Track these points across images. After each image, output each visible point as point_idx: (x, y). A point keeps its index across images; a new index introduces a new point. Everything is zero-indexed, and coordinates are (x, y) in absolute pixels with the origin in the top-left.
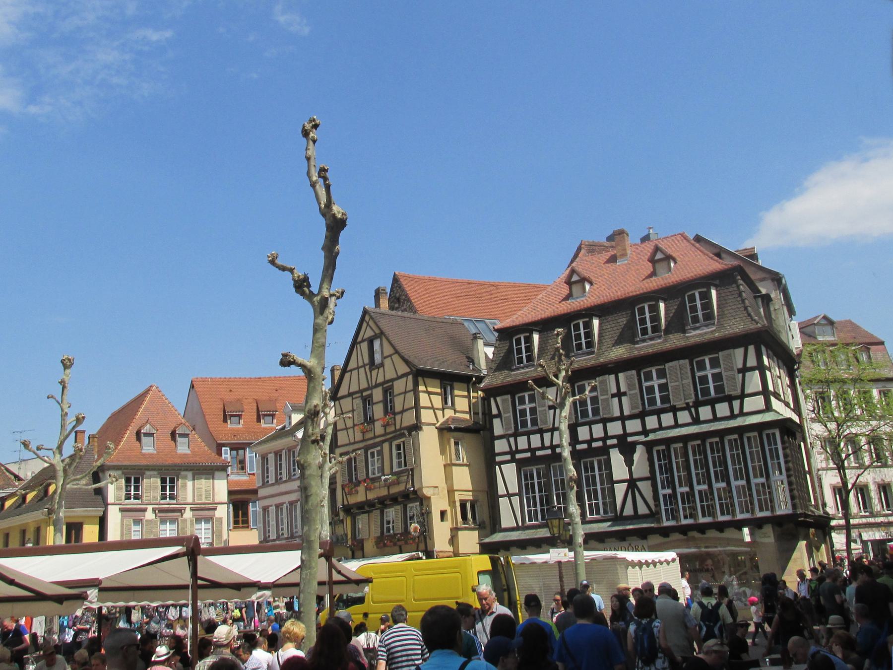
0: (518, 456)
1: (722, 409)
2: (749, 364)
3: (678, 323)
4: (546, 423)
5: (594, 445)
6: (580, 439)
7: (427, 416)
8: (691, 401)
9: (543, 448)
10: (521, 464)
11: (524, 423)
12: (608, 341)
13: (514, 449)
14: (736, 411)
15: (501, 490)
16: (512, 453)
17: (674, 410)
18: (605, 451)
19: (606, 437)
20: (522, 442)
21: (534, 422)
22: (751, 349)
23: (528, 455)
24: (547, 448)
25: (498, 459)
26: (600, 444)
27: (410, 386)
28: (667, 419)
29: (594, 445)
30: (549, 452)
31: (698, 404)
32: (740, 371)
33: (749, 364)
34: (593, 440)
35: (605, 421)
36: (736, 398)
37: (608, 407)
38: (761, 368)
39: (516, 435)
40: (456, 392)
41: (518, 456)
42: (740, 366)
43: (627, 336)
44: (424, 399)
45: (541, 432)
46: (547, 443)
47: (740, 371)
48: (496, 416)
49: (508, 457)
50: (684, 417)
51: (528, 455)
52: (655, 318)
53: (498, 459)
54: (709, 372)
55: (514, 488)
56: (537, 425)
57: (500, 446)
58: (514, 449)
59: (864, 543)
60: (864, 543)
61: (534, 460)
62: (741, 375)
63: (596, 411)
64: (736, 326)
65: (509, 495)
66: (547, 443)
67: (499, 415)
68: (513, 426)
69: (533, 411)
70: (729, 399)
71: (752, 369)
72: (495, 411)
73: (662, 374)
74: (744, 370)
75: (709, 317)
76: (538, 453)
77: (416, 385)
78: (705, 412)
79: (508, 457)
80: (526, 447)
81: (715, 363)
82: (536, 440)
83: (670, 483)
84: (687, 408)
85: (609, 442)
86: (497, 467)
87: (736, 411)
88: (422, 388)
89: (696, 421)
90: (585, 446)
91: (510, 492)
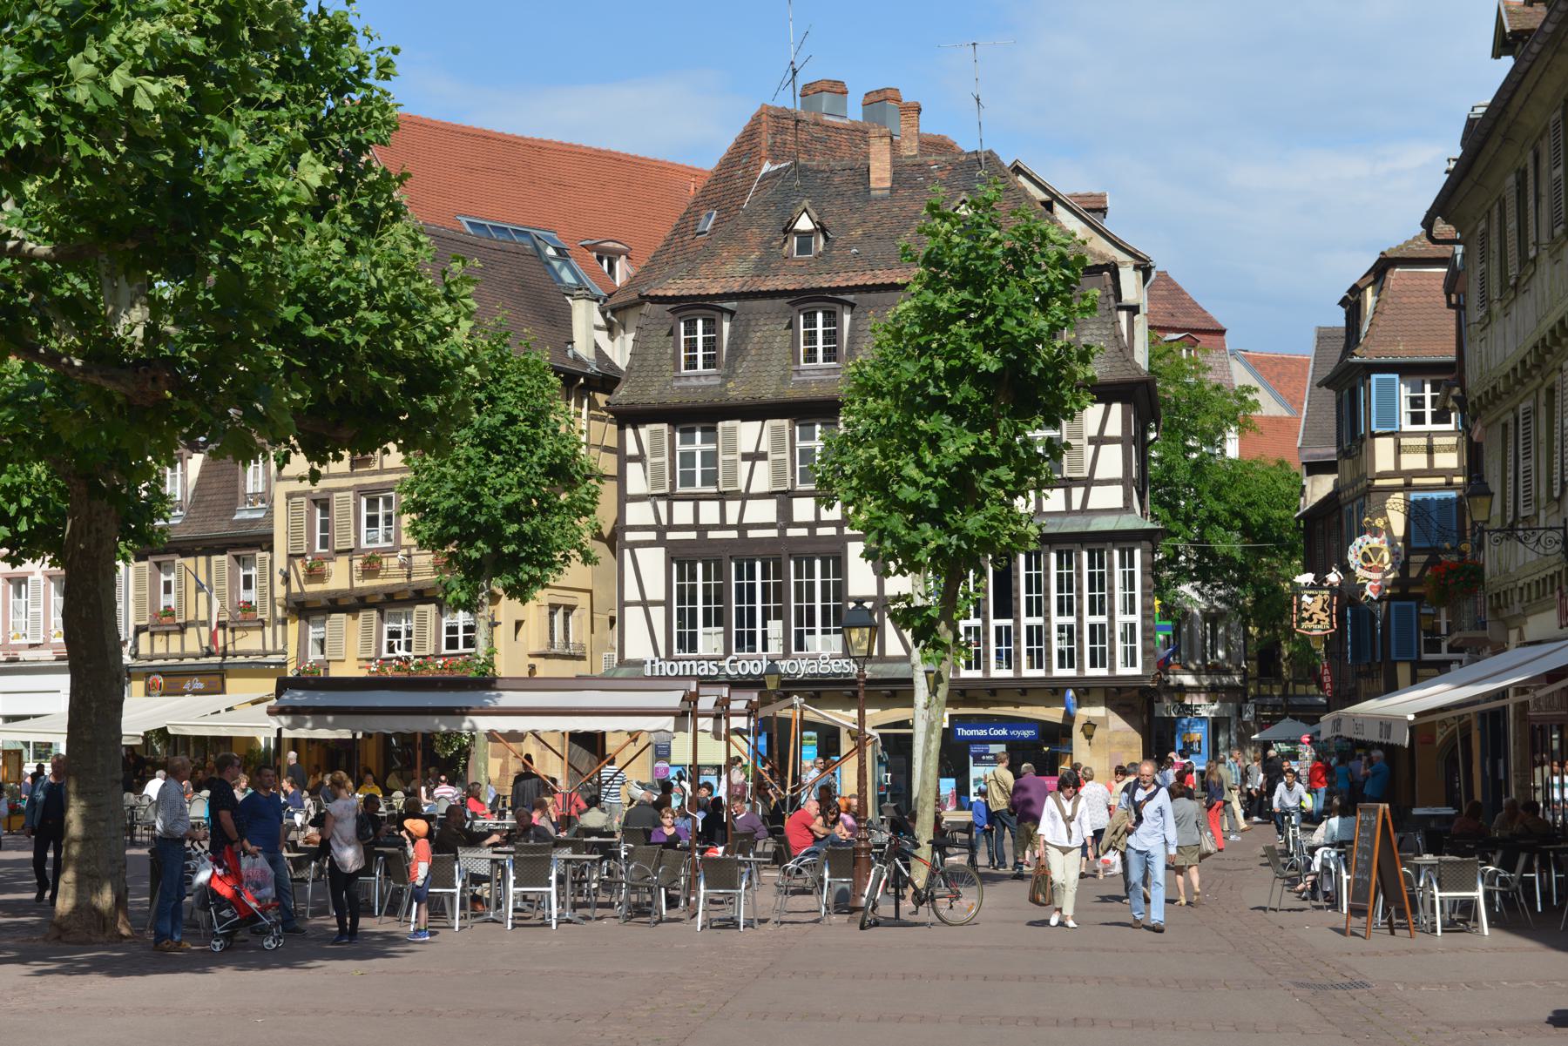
0: (671, 536)
2: (1108, 432)
4: (734, 482)
5: (821, 531)
6: (797, 518)
9: (723, 526)
11: (688, 479)
13: (664, 521)
14: (1076, 505)
16: (660, 529)
20: (683, 513)
21: (710, 479)
23: (693, 535)
24: (731, 527)
26: (832, 531)
29: (821, 531)
30: (734, 534)
32: (1091, 441)
33: (1108, 432)
34: (819, 523)
39: (671, 498)
41: (671, 536)
42: (1093, 431)
45: (722, 497)
46: (732, 519)
47: (1091, 441)
49: (652, 536)
51: (693, 535)
53: (630, 536)
55: (656, 591)
56: (716, 483)
58: (664, 521)
62: (1092, 448)
65: (645, 604)
66: (732, 519)
67: (640, 458)
68: (667, 480)
69: (710, 458)
76: (712, 535)
79: (652, 536)
80: (690, 521)
82: (710, 512)
86: (627, 552)
87: (1076, 505)
90: (804, 532)
91: (649, 597)
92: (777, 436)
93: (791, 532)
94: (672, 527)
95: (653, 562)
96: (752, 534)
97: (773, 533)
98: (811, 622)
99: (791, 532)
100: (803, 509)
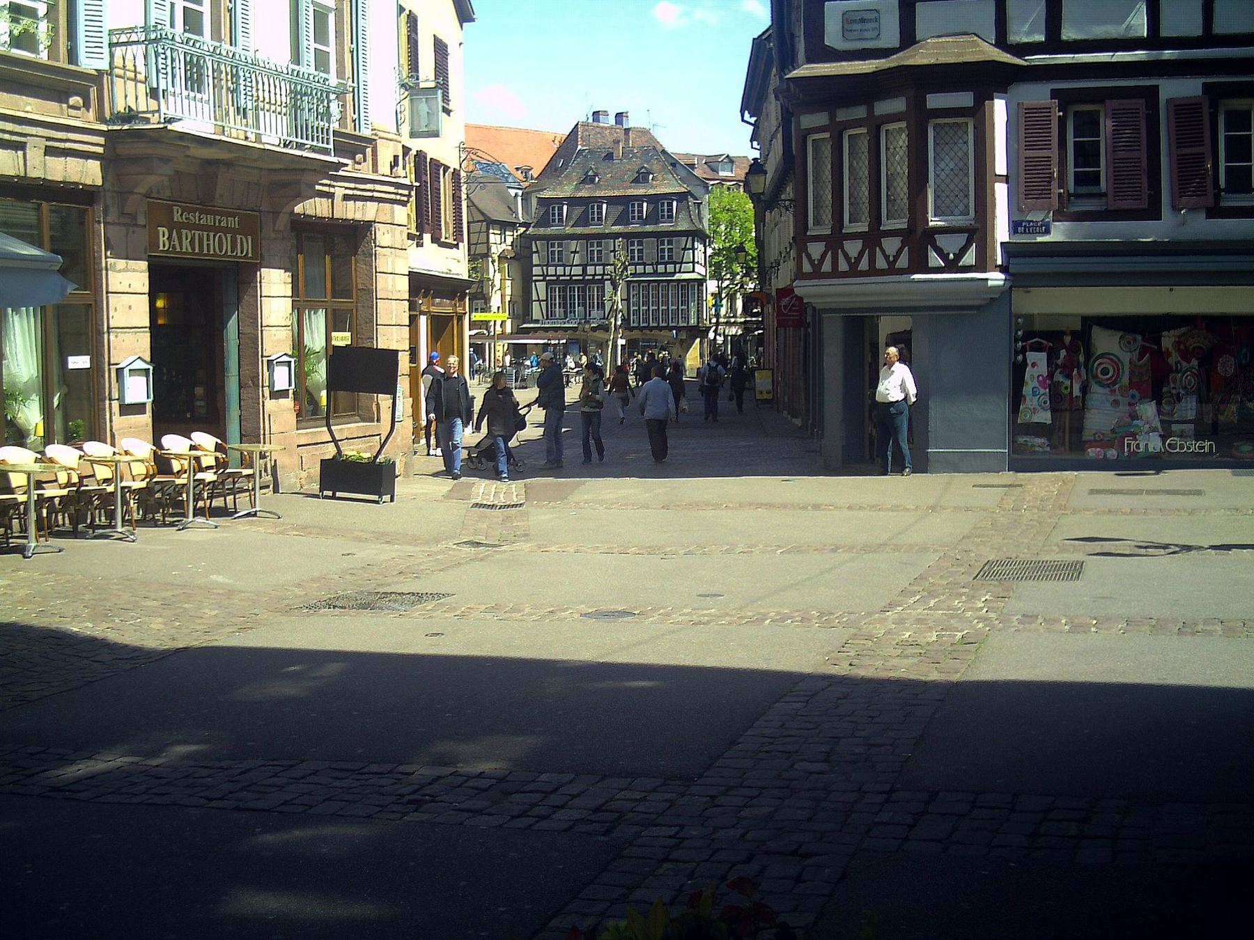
0: (548, 278)
1: (670, 268)
3: (654, 218)
5: (596, 277)
7: (494, 249)
8: (654, 262)
9: (564, 275)
10: (549, 283)
11: (553, 260)
12: (611, 221)
14: (677, 270)
15: (535, 297)
17: (645, 264)
18: (602, 281)
19: (604, 274)
20: (551, 270)
22: (690, 238)
23: (555, 278)
25: (534, 278)
26: (600, 277)
27: (484, 229)
28: (640, 269)
29: (596, 277)
30: (568, 278)
31: (658, 263)
32: (683, 249)
34: (595, 275)
35: (604, 265)
36: (678, 263)
37: (607, 256)
38: (693, 249)
39: (547, 266)
40: (507, 233)
41: (548, 278)
43: (622, 219)
44: (492, 237)
45: (564, 266)
48: (535, 252)
49: (542, 278)
50: (649, 269)
51: (555, 278)
52: (641, 211)
54: (666, 247)
55: (543, 296)
57: (536, 270)
59: (726, 336)
60: (726, 336)
61: (557, 282)
63: (599, 259)
64: (683, 226)
70: (675, 263)
71: (689, 249)
72: (534, 249)
73: (640, 243)
74: (685, 249)
75: (670, 217)
76: (561, 278)
77: (488, 229)
78: (661, 268)
79: (542, 278)
81: (670, 243)
82: (560, 270)
83: (646, 303)
84: (652, 264)
85: (605, 277)
87: (677, 270)
88: (491, 231)
89: (655, 273)
90: (591, 277)
92: (581, 244)
93: (587, 278)
94: (547, 275)
95: (541, 286)
96: (574, 278)
97: (581, 278)
98: (593, 307)
99: (587, 278)
100: (590, 270)
